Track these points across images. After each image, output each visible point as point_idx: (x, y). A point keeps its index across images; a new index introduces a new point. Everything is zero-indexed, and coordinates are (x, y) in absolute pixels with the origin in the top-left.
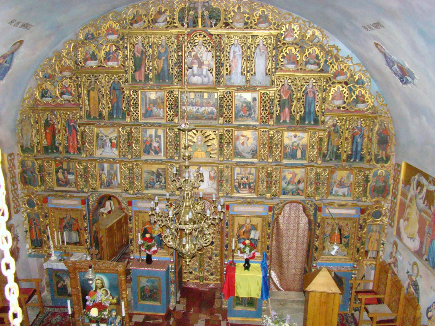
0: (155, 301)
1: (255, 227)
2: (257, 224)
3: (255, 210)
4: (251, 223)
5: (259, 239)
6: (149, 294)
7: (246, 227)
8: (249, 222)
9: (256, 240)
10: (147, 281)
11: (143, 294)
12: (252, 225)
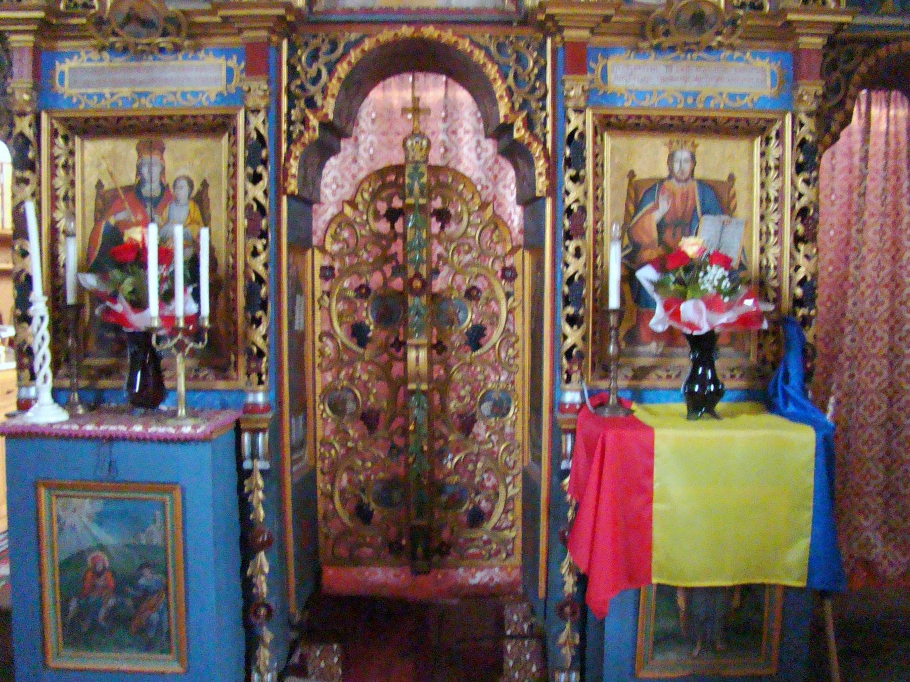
0: (149, 647)
1: (718, 197)
2: (731, 178)
4: (698, 174)
6: (111, 602)
7: (673, 195)
8: (687, 167)
10: (101, 519)
11: (73, 605)
12: (701, 182)
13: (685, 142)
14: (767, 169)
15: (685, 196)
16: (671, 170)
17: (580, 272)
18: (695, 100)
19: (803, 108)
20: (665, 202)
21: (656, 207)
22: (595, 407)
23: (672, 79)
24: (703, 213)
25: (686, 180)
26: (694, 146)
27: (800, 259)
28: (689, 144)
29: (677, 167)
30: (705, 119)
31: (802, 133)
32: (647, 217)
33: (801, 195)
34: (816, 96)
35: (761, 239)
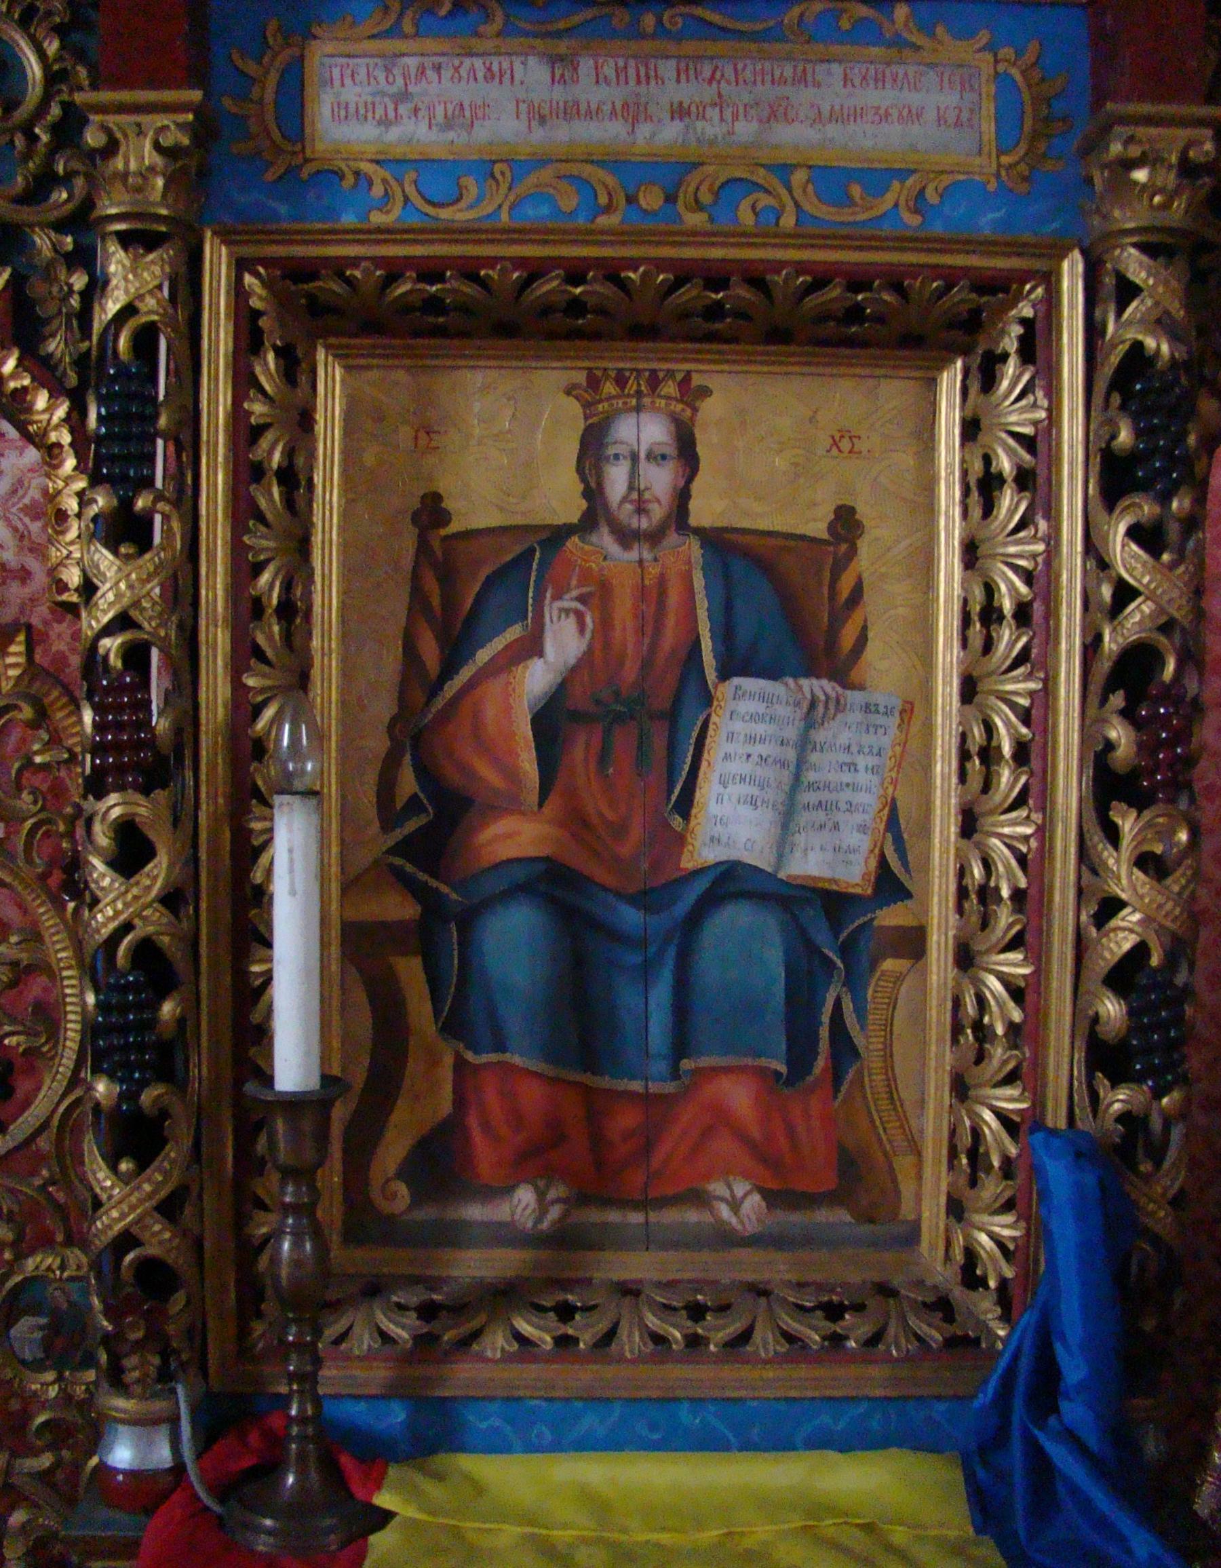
1: (790, 605)
2: (846, 523)
3: (793, 136)
4: (707, 509)
5: (889, 885)
7: (599, 595)
8: (660, 480)
9: (834, 902)
12: (721, 545)
13: (655, 382)
14: (986, 486)
15: (653, 597)
16: (594, 493)
17: (141, 930)
18: (671, 199)
19: (1126, 218)
20: (570, 624)
21: (532, 647)
22: (222, 1492)
23: (571, 111)
24: (725, 674)
25: (654, 537)
26: (691, 394)
27: (1123, 877)
28: (670, 388)
29: (617, 479)
30: (716, 277)
31: (1128, 328)
32: (494, 688)
33: (1125, 594)
34: (1187, 169)
35: (963, 777)
